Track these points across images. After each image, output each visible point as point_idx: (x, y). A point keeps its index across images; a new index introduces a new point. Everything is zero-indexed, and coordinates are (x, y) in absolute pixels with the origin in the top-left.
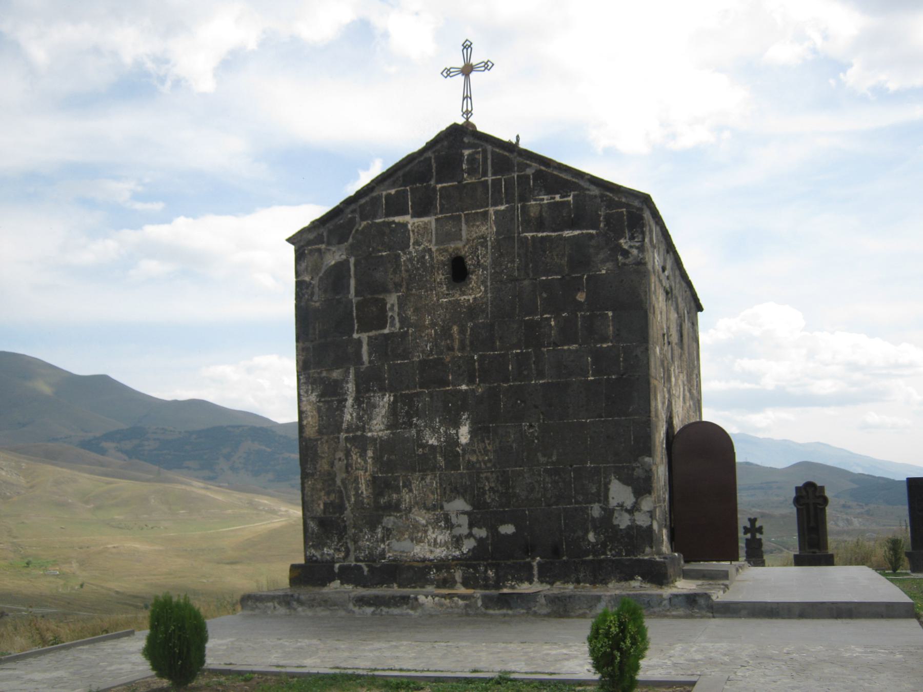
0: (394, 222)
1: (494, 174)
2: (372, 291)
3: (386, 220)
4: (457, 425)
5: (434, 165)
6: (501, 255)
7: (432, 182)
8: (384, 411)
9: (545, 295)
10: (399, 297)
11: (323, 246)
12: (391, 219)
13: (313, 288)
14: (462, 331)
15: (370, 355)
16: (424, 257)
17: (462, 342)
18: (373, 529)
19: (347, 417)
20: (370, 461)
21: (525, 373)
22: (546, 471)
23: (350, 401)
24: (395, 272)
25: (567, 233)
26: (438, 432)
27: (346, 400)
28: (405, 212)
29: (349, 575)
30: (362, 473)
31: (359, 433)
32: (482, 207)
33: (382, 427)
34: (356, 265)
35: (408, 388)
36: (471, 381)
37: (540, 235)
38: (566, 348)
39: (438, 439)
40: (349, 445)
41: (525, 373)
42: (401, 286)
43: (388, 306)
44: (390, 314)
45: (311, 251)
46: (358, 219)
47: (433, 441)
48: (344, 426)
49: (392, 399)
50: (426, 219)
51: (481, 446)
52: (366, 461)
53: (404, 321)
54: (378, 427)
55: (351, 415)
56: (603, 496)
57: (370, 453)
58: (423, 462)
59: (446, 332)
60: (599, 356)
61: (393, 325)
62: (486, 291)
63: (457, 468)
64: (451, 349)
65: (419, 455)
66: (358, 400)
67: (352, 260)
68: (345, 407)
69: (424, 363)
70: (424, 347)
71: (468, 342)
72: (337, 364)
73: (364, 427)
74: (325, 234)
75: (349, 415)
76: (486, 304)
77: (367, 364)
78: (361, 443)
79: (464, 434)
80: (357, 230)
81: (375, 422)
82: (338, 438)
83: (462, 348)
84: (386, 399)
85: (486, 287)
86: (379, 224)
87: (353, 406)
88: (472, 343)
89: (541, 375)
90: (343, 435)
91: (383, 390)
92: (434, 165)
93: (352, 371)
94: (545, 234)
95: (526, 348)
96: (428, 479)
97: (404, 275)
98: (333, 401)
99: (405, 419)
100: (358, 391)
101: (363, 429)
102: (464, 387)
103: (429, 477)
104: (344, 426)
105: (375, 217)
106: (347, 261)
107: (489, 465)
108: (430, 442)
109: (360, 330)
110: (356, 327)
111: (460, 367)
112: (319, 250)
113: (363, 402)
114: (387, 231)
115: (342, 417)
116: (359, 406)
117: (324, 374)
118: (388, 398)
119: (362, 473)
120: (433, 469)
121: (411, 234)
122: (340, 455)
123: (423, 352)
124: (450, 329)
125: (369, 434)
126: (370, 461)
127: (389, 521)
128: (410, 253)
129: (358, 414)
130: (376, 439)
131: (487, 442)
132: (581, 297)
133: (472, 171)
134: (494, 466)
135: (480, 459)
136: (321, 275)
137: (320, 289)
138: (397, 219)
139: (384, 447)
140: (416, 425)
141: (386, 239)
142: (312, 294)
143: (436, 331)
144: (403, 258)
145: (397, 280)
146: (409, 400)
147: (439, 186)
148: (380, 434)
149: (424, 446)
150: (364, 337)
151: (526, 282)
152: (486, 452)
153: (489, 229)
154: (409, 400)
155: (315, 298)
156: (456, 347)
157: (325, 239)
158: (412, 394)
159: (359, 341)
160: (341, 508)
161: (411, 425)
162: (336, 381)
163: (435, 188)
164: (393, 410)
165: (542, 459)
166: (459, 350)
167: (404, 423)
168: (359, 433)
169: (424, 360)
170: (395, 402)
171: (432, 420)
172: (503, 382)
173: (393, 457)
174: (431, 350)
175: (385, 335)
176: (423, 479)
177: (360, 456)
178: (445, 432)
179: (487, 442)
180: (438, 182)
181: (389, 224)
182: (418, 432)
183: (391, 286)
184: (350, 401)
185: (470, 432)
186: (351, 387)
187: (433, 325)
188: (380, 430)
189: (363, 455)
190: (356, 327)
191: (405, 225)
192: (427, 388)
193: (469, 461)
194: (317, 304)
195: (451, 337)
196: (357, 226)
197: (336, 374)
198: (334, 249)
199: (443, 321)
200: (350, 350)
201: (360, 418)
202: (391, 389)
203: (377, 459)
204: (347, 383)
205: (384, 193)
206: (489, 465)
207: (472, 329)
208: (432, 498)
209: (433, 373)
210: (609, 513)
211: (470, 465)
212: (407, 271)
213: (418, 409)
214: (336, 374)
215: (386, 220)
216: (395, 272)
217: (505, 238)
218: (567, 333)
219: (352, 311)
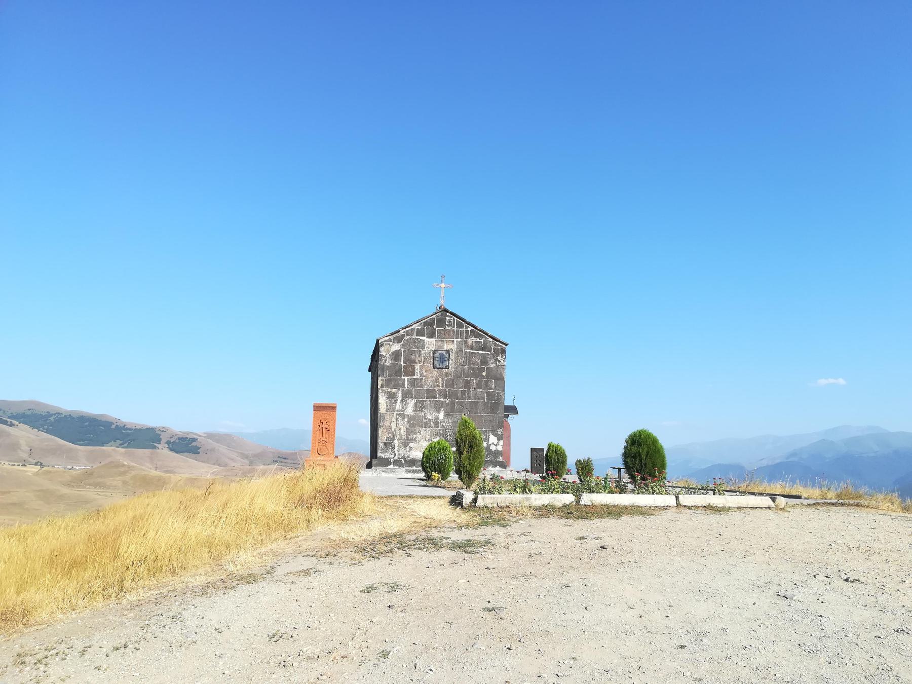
2: (410, 362)
4: (439, 412)
18: (405, 447)
25: (481, 352)
29: (397, 463)
53: (421, 374)
54: (410, 410)
56: (487, 440)
58: (426, 425)
59: (437, 380)
60: (489, 394)
70: (428, 384)
72: (395, 387)
75: (398, 405)
78: (402, 416)
79: (441, 416)
89: (469, 398)
109: (405, 375)
118: (414, 401)
122: (394, 419)
127: (411, 445)
132: (484, 374)
139: (411, 418)
150: (406, 378)
153: (453, 347)
160: (393, 439)
164: (416, 406)
186: (400, 396)
197: (394, 390)
203: (409, 422)
208: (428, 437)
209: (431, 394)
210: (489, 445)
214: (394, 390)
217: (460, 351)
218: (479, 386)
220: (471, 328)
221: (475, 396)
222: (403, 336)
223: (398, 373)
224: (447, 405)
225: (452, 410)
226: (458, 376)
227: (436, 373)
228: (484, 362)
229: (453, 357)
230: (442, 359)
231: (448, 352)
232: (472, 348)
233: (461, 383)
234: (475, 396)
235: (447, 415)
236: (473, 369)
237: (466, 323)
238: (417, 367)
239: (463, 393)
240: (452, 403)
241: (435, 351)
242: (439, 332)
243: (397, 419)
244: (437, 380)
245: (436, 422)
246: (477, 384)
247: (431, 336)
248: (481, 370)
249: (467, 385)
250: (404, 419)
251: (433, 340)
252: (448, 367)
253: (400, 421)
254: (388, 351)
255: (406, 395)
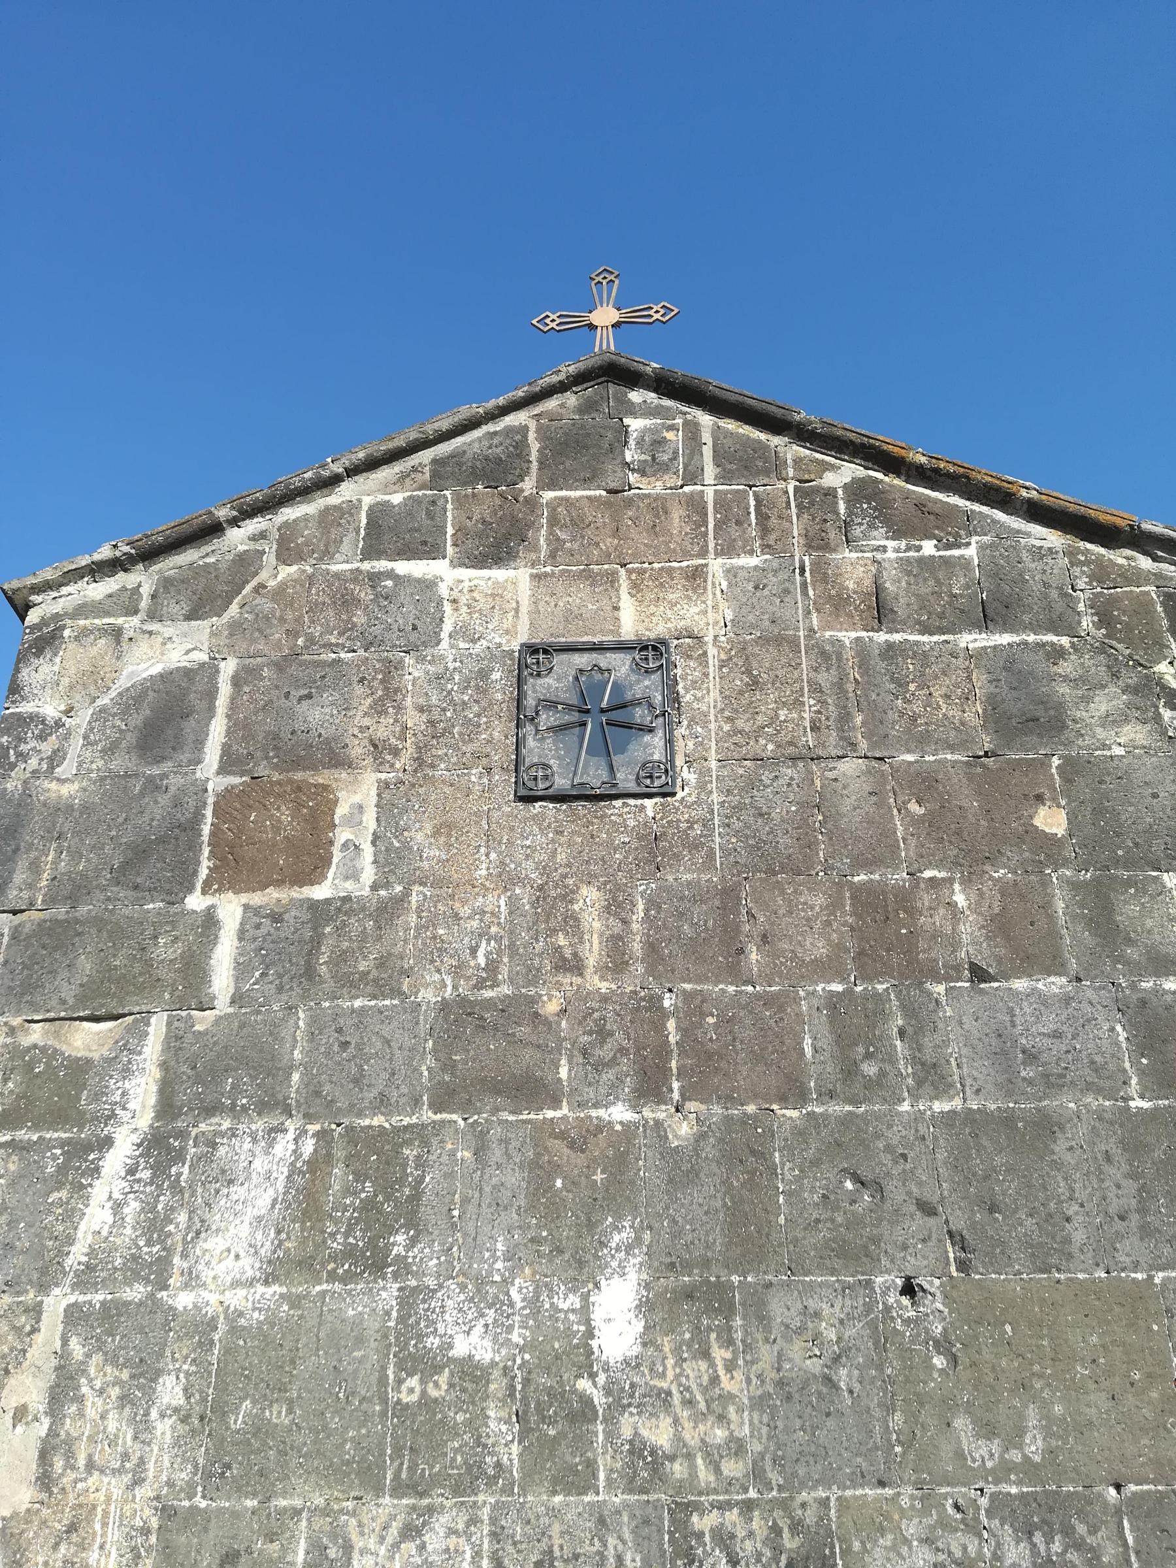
0: (391, 574)
1: (724, 477)
3: (366, 566)
4: (584, 1270)
5: (534, 446)
6: (755, 684)
7: (528, 486)
8: (264, 1201)
9: (914, 807)
10: (384, 786)
11: (129, 624)
12: (383, 565)
13: (67, 737)
14: (616, 907)
15: (241, 970)
16: (484, 674)
17: (616, 947)
19: (96, 1217)
20: (164, 1429)
21: (870, 1069)
22: (999, 1505)
23: (124, 1146)
24: (378, 709)
26: (501, 1303)
27: (107, 1143)
28: (433, 551)
30: (116, 1486)
31: (136, 1292)
32: (687, 555)
33: (248, 1267)
34: (236, 681)
35: (382, 1104)
36: (650, 1087)
37: (882, 637)
38: (1020, 984)
39: (498, 1332)
40: (77, 1348)
41: (870, 1069)
42: (396, 752)
43: (341, 811)
44: (342, 835)
45: (84, 633)
46: (270, 559)
47: (473, 1344)
48: (77, 1255)
49: (308, 1147)
50: (499, 574)
51: (696, 1370)
52: (142, 1429)
53: (393, 858)
54: (228, 1266)
55: (117, 1207)
57: (170, 1391)
59: (552, 906)
61: (353, 875)
62: (702, 786)
63: (578, 1480)
64: (575, 966)
65: (402, 1409)
66: (160, 1149)
67: (228, 668)
68: (95, 1171)
69: (460, 1016)
70: (460, 947)
71: (637, 947)
73: (162, 1265)
74: (146, 591)
75: (105, 1209)
76: (706, 823)
77: (223, 1005)
79: (616, 1314)
80: (262, 586)
81: (213, 1244)
82: (36, 1311)
83: (616, 963)
84: (283, 1146)
85: (704, 773)
86: (337, 575)
87: (132, 1171)
88: (652, 948)
89: (932, 1077)
90: (57, 1301)
91: (272, 1103)
92: (534, 446)
93: (157, 1026)
94: (897, 637)
95: (866, 976)
96: (435, 1540)
97: (413, 719)
98: (48, 1145)
99: (358, 1239)
100: (167, 1107)
101: (158, 1273)
102: (619, 1113)
103: (441, 1522)
104: (77, 1255)
105: (327, 554)
106: (210, 670)
107: (732, 1468)
108: (461, 1348)
109: (220, 882)
110: (203, 872)
111: (603, 1034)
112: (117, 633)
113: (180, 1157)
114: (366, 595)
115: (71, 1216)
116: (160, 1170)
117: (36, 1035)
118: (293, 1144)
119: (116, 1486)
120: (464, 1485)
121: (447, 607)
123: (458, 971)
124: (568, 896)
125: (184, 1300)
126: (164, 1429)
128: (438, 659)
129: (149, 1207)
130: (212, 1325)
131: (720, 1354)
133: (652, 468)
134: (757, 1474)
135: (691, 1436)
136: (104, 701)
137: (88, 743)
138: (403, 567)
139: (242, 1363)
140: (403, 1268)
141: (360, 618)
142: (56, 759)
143: (513, 903)
144: (414, 671)
145: (381, 733)
146: (379, 1157)
147: (548, 495)
148: (237, 1299)
149: (425, 1364)
150: (230, 909)
151: (849, 767)
152: (717, 1406)
153: (704, 615)
154: (379, 1157)
155: (66, 769)
156: (591, 961)
157: (144, 604)
158: (397, 1130)
159: (210, 922)
161: (374, 1262)
162: (80, 1068)
163: (532, 503)
164: (306, 1199)
165: (984, 1452)
166: (602, 971)
167: (349, 1253)
168: (136, 1292)
169: (462, 1002)
170: (318, 1165)
171: (474, 1246)
172: (783, 1100)
173: (278, 1415)
174: (492, 967)
175: (314, 906)
176: (410, 1532)
177: (124, 1399)
178: (533, 1302)
179: (720, 1354)
180: (542, 486)
181: (374, 578)
182: (407, 1300)
183: (357, 749)
184: (124, 1146)
185: (646, 1307)
186: (140, 1095)
187: (506, 880)
188: (236, 1284)
189: (136, 1397)
190: (203, 872)
191: (428, 585)
192: (466, 1107)
193: (637, 1448)
194: (66, 790)
195: (572, 924)
196: (263, 575)
198: (168, 630)
199: (545, 870)
200: (165, 950)
201: (154, 1226)
202: (315, 1104)
203: (204, 1418)
204: (126, 1073)
205: (367, 501)
206: (732, 1468)
207: (651, 903)
211: (645, 1466)
212: (421, 710)
213: (416, 1197)
214: (86, 1039)
215: (366, 566)
216: (378, 709)
217: (760, 649)
218: (1022, 940)
219: (198, 817)
220: (842, 474)
221: (1005, 1051)
222: (246, 564)
223: (158, 857)
224: (681, 1169)
225: (748, 1236)
226: (774, 863)
227: (542, 835)
228: (1026, 715)
229: (704, 691)
230: (607, 719)
231: (651, 651)
232: (880, 611)
233: (812, 922)
234: (1005, 1051)
235: (688, 1303)
236: (924, 783)
237: (802, 434)
238: (357, 797)
239: (852, 1025)
240: (744, 1150)
241: (537, 654)
242: (572, 519)
243: (63, 1389)
244: (552, 906)
245: (557, 1407)
246: (999, 926)
247: (495, 546)
248: (1005, 787)
249: (886, 934)
250: (146, 1373)
251: (516, 578)
252: (658, 783)
253: (98, 1409)
254: (93, 679)
255: (204, 1086)
